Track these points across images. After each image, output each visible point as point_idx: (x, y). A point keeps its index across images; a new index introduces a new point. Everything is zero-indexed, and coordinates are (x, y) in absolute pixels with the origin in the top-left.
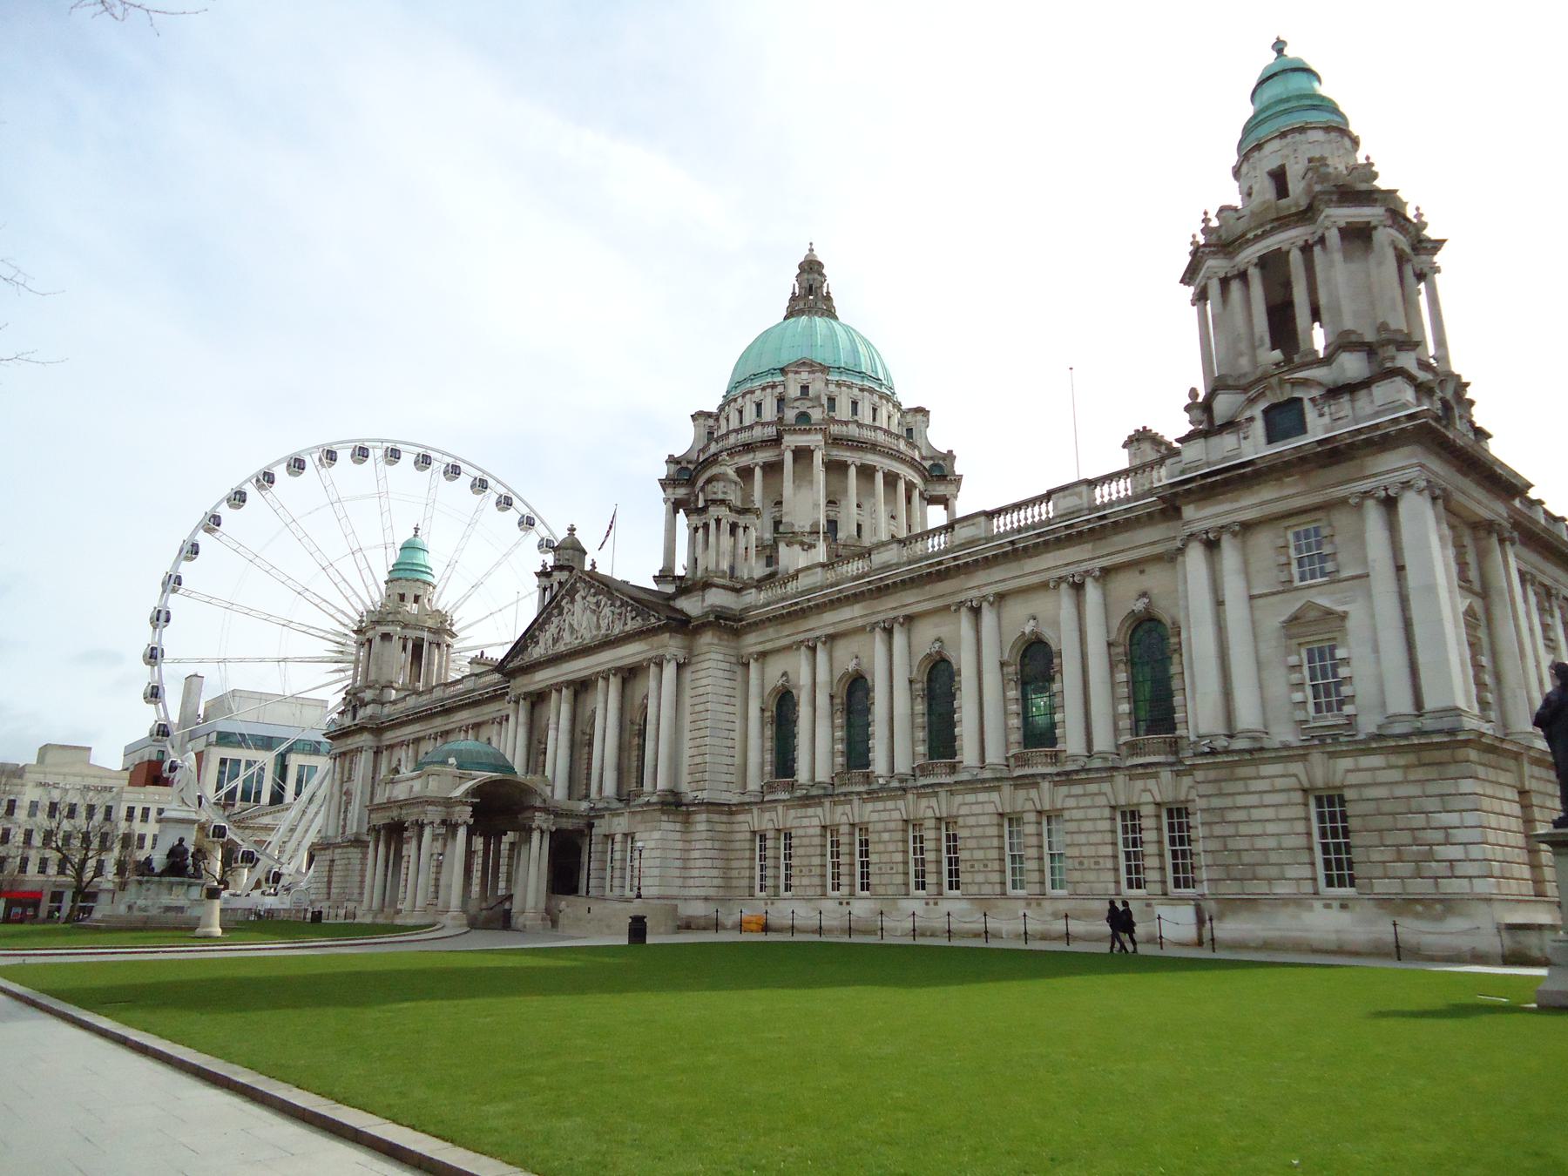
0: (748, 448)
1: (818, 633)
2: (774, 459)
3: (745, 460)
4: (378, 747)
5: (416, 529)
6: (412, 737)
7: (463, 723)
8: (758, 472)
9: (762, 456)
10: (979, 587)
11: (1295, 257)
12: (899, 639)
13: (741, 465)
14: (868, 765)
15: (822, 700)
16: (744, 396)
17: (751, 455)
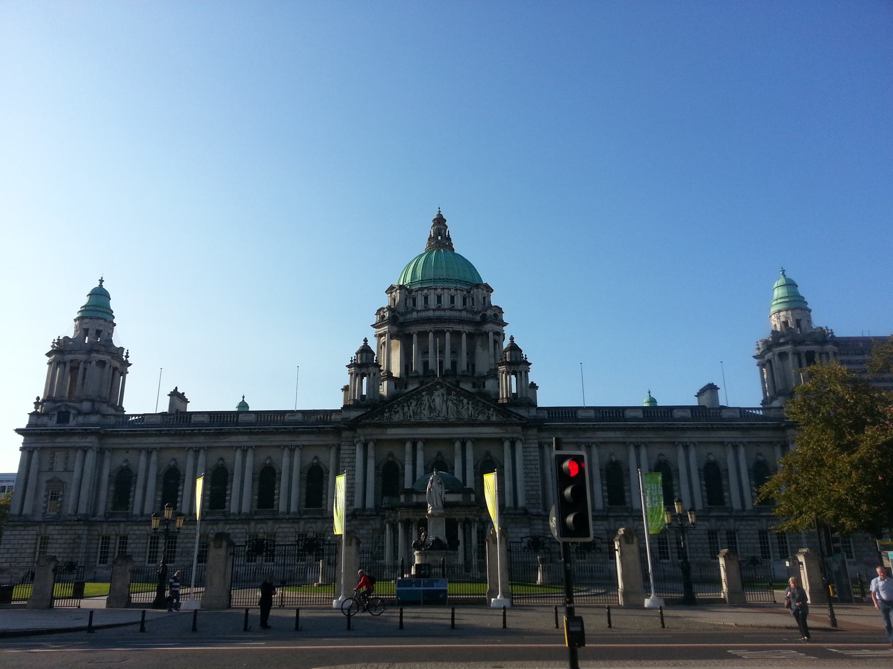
0: (461, 321)
1: (593, 440)
2: (473, 332)
3: (457, 327)
4: (101, 449)
5: (101, 281)
6: (158, 446)
7: (243, 444)
8: (464, 336)
9: (467, 329)
10: (689, 438)
11: (817, 356)
12: (643, 452)
13: (455, 329)
14: (624, 503)
15: (596, 471)
16: (443, 289)
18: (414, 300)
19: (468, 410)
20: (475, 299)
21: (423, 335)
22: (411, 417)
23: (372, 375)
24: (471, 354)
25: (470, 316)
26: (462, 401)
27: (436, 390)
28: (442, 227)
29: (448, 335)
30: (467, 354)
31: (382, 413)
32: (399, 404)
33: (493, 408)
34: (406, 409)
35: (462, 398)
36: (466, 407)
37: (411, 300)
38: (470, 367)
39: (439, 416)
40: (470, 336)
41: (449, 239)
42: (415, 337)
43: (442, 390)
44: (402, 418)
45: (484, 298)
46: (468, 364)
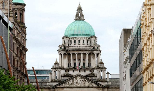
0: (86, 50)
2: (90, 53)
3: (85, 52)
8: (87, 55)
9: (88, 52)
16: (81, 38)
17: (86, 52)
18: (71, 41)
19: (87, 83)
20: (91, 41)
21: (74, 54)
22: (71, 85)
23: (59, 71)
24: (89, 60)
25: (89, 47)
26: (85, 80)
27: (78, 77)
28: (81, 11)
29: (82, 55)
30: (88, 60)
31: (62, 84)
32: (67, 81)
33: (95, 83)
34: (69, 83)
35: (85, 80)
36: (86, 82)
37: (70, 41)
38: (89, 64)
39: (79, 85)
40: (89, 54)
41: (83, 15)
42: (71, 55)
43: (80, 77)
44: (68, 85)
45: (94, 41)
46: (88, 63)
